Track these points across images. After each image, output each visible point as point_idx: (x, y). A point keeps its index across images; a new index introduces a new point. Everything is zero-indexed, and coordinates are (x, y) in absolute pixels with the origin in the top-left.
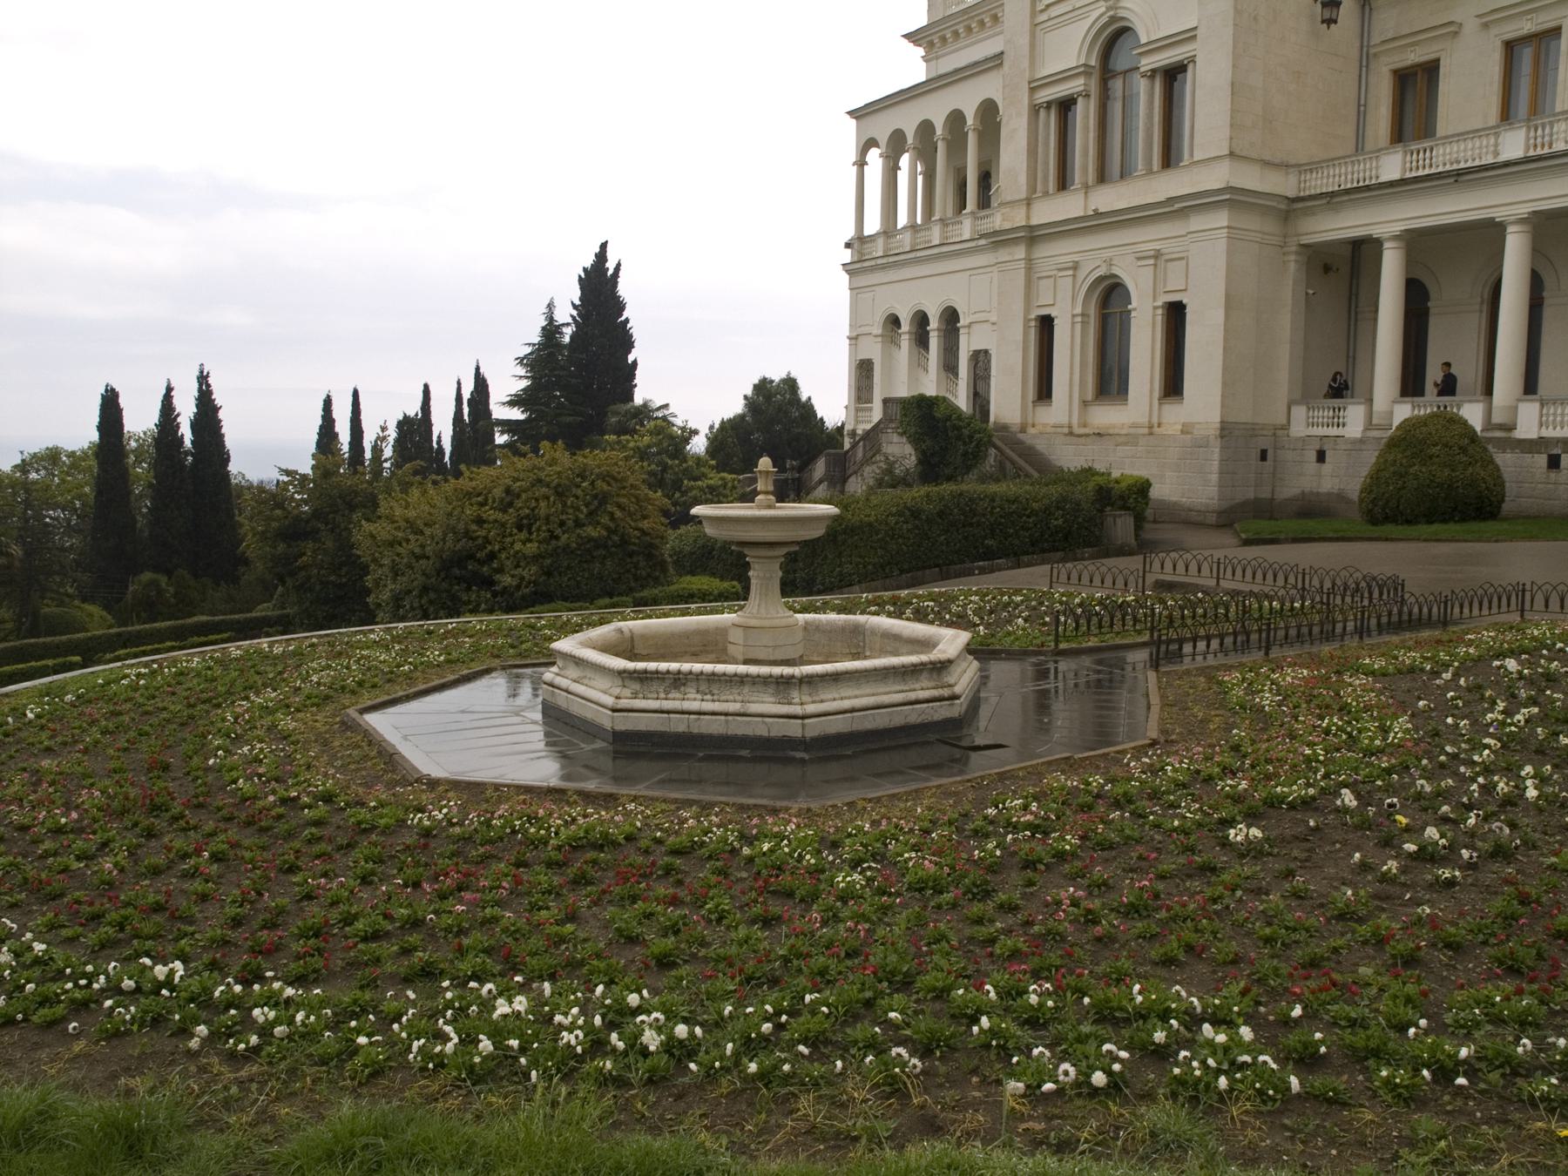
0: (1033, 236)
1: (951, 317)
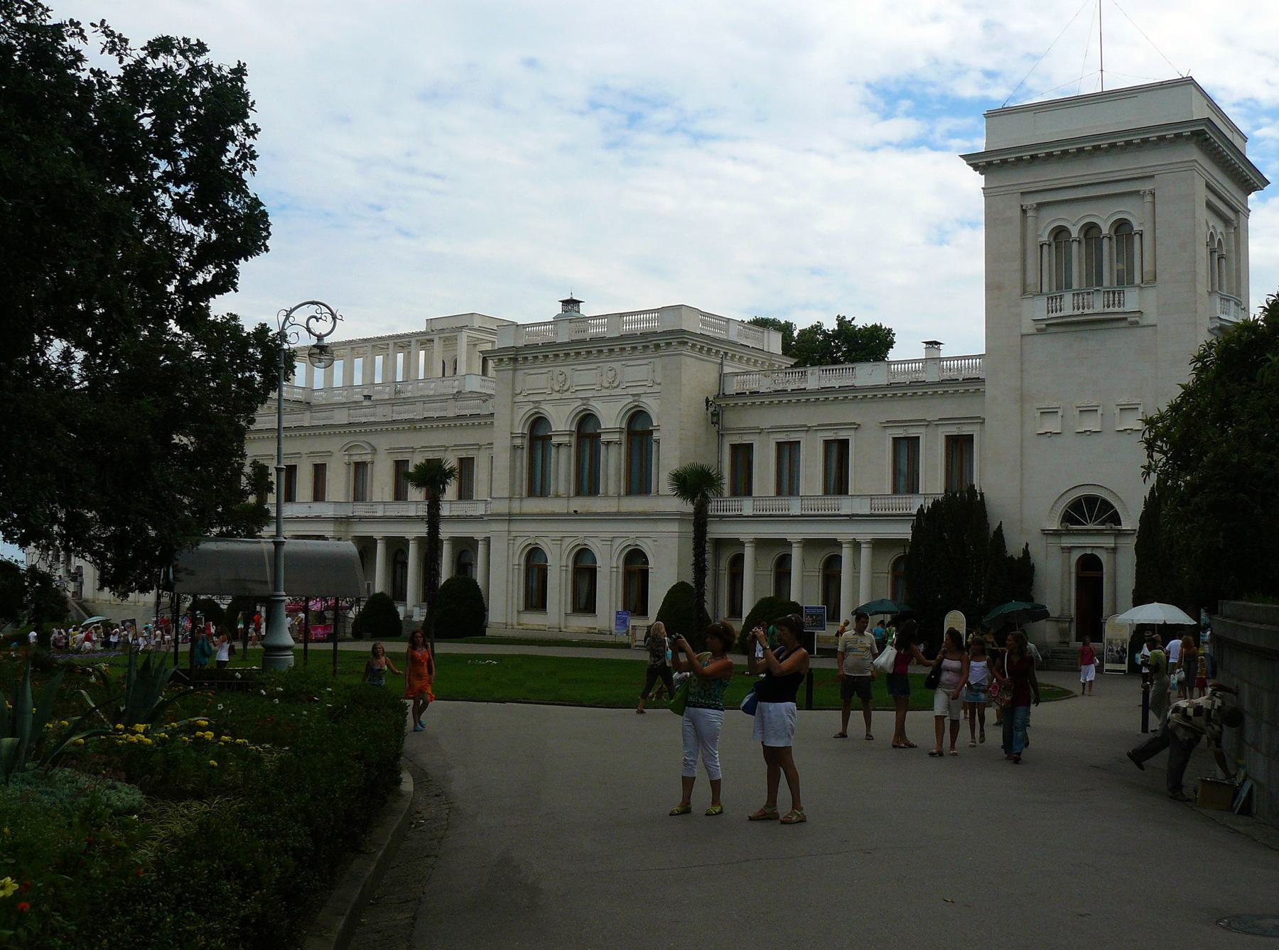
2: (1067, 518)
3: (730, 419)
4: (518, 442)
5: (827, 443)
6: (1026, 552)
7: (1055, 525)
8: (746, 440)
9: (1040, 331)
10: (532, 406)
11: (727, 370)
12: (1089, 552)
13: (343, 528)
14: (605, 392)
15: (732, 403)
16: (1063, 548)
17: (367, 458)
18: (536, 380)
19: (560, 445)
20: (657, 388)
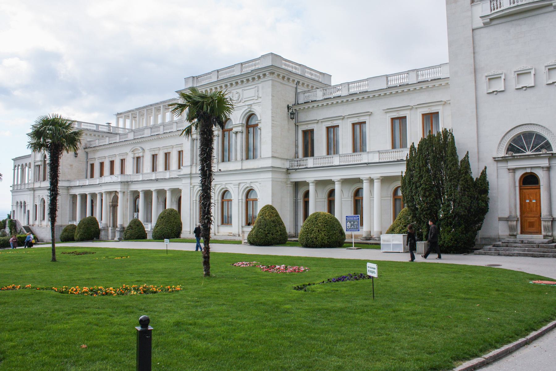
0: (34, 190)
1: (25, 203)
2: (511, 148)
3: (302, 117)
6: (484, 174)
7: (502, 154)
8: (309, 127)
9: (486, 25)
11: (299, 91)
12: (529, 171)
13: (126, 187)
15: (302, 107)
16: (509, 169)
17: (141, 155)
20: (260, 100)
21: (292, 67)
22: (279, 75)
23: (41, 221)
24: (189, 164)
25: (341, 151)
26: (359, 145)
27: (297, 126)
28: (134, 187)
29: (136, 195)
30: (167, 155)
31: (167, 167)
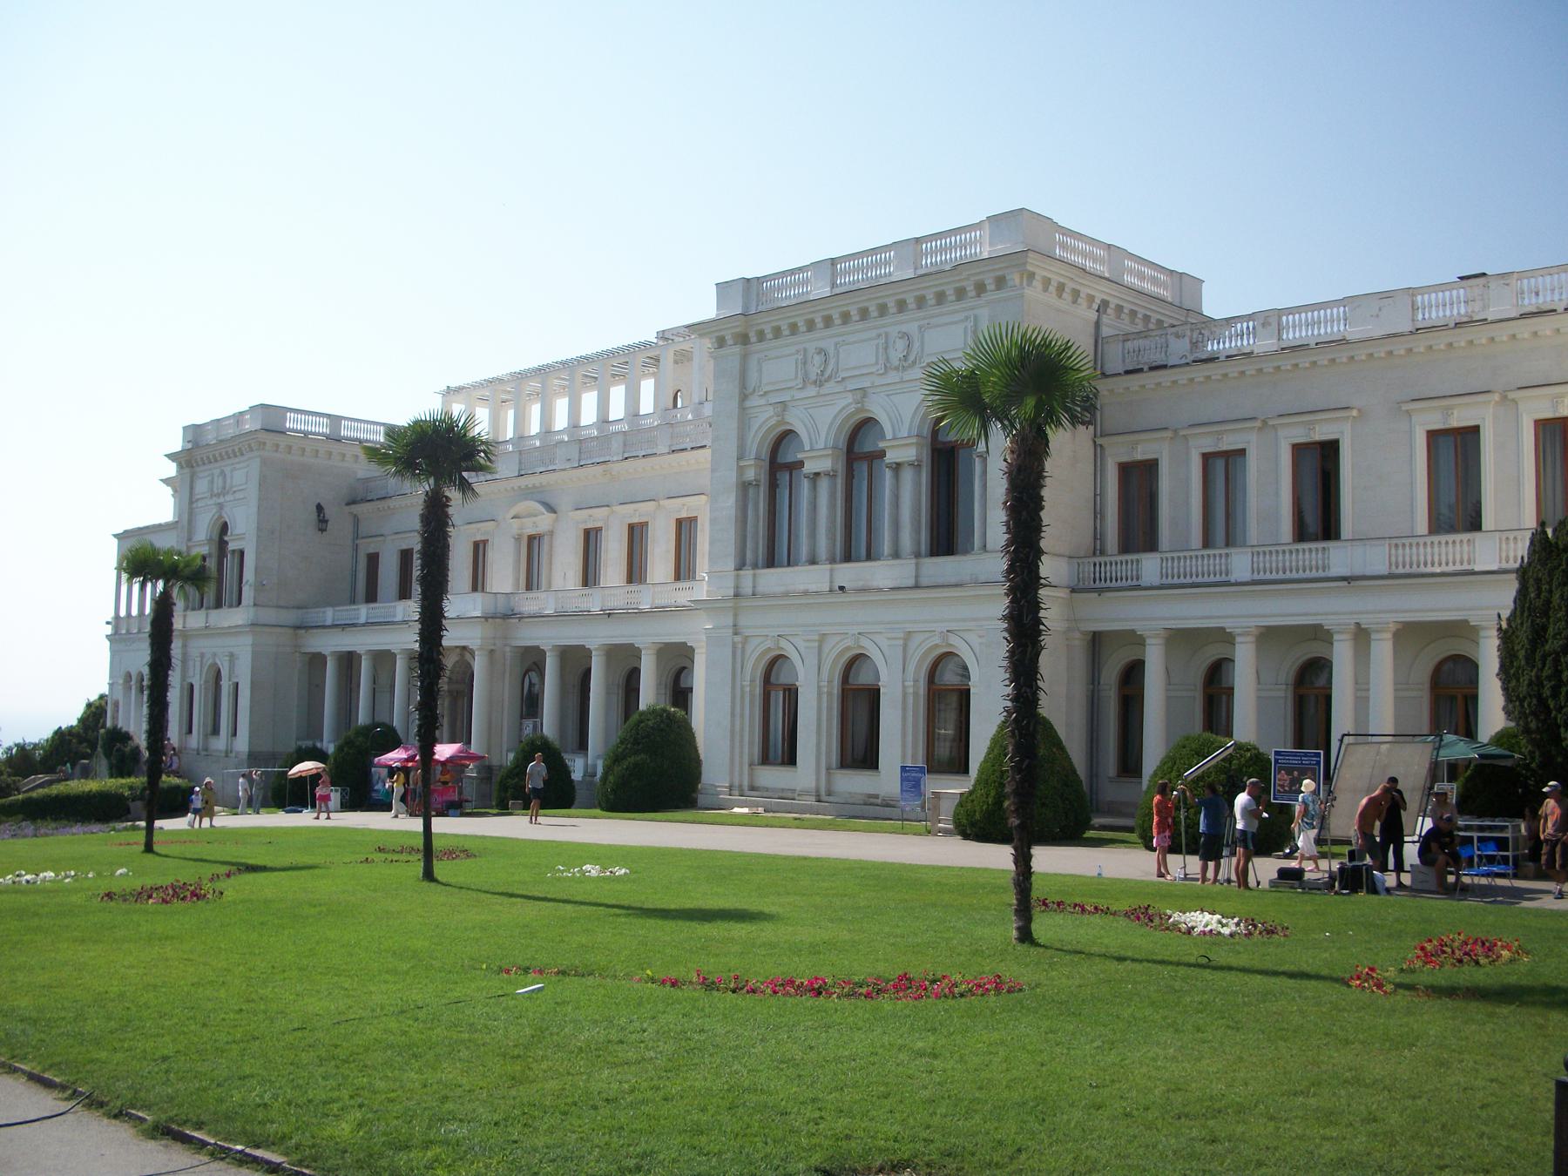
4: (750, 475)
5: (1298, 450)
10: (770, 411)
14: (893, 377)
18: (777, 367)
19: (817, 474)
21: (1084, 255)
22: (1047, 282)
23: (206, 736)
24: (730, 564)
25: (1253, 530)
26: (1320, 515)
27: (1099, 451)
28: (530, 636)
29: (532, 661)
30: (636, 535)
31: (635, 572)
